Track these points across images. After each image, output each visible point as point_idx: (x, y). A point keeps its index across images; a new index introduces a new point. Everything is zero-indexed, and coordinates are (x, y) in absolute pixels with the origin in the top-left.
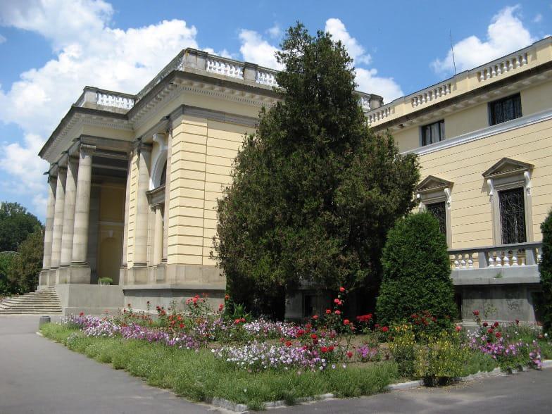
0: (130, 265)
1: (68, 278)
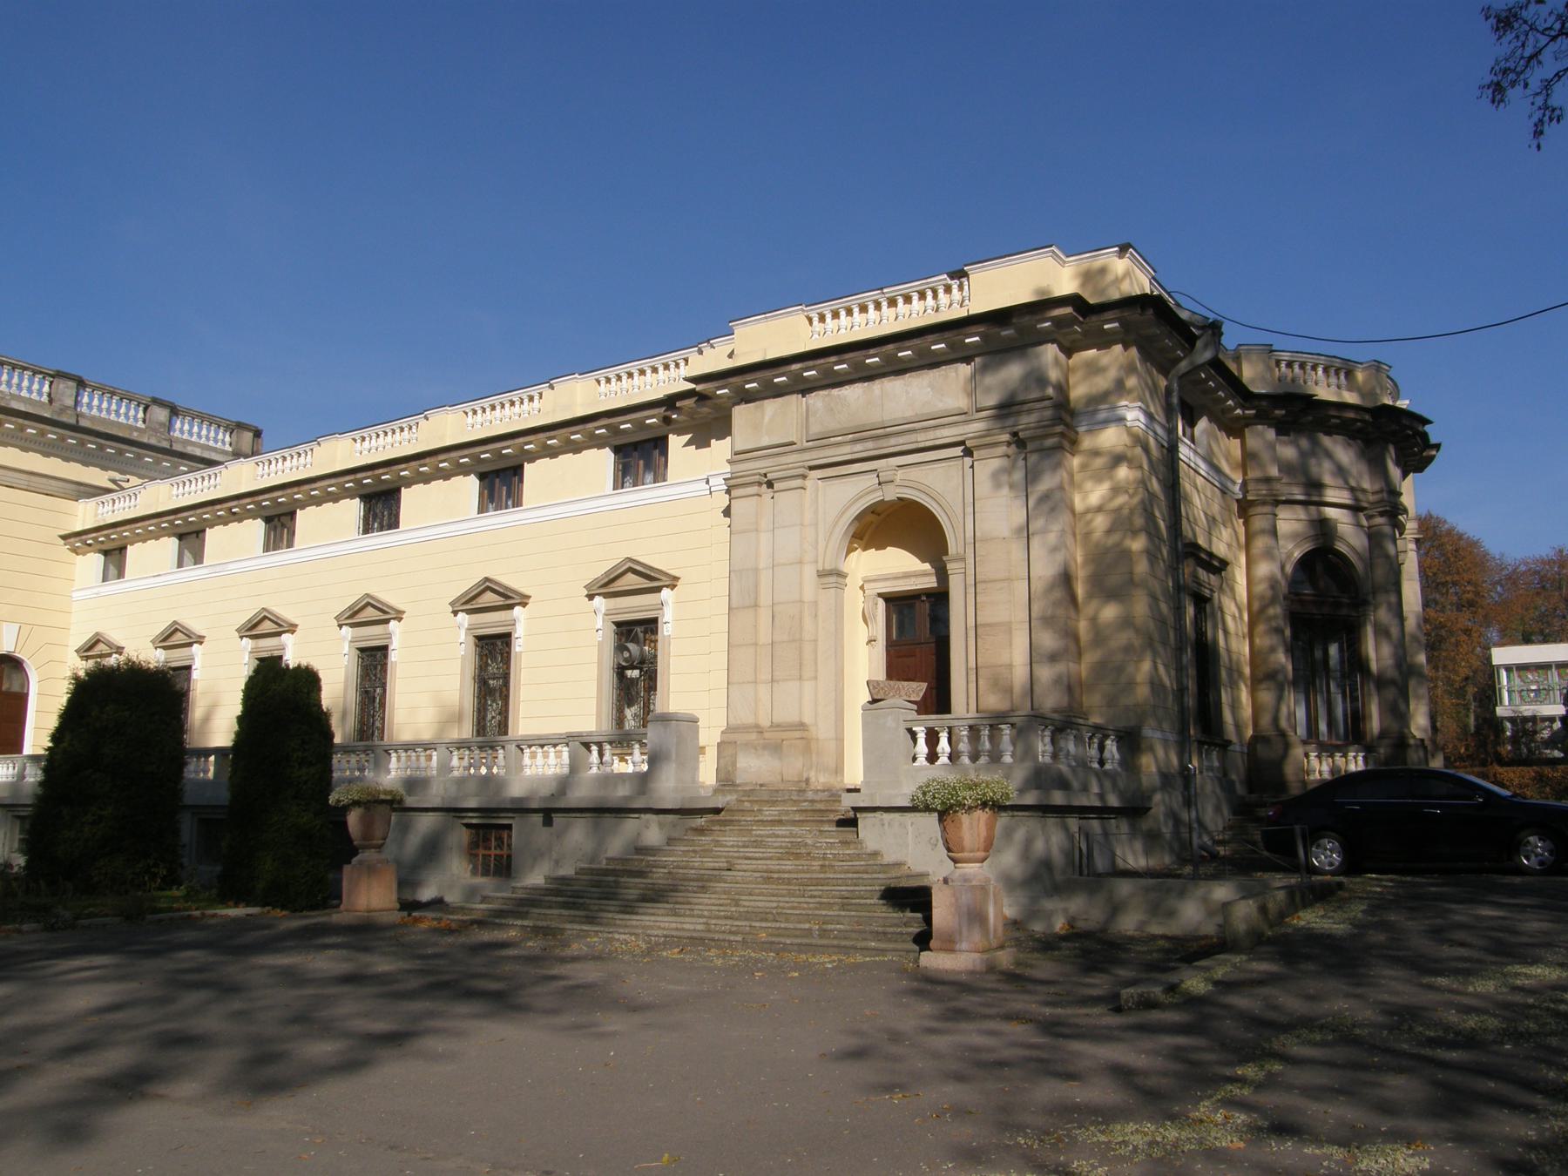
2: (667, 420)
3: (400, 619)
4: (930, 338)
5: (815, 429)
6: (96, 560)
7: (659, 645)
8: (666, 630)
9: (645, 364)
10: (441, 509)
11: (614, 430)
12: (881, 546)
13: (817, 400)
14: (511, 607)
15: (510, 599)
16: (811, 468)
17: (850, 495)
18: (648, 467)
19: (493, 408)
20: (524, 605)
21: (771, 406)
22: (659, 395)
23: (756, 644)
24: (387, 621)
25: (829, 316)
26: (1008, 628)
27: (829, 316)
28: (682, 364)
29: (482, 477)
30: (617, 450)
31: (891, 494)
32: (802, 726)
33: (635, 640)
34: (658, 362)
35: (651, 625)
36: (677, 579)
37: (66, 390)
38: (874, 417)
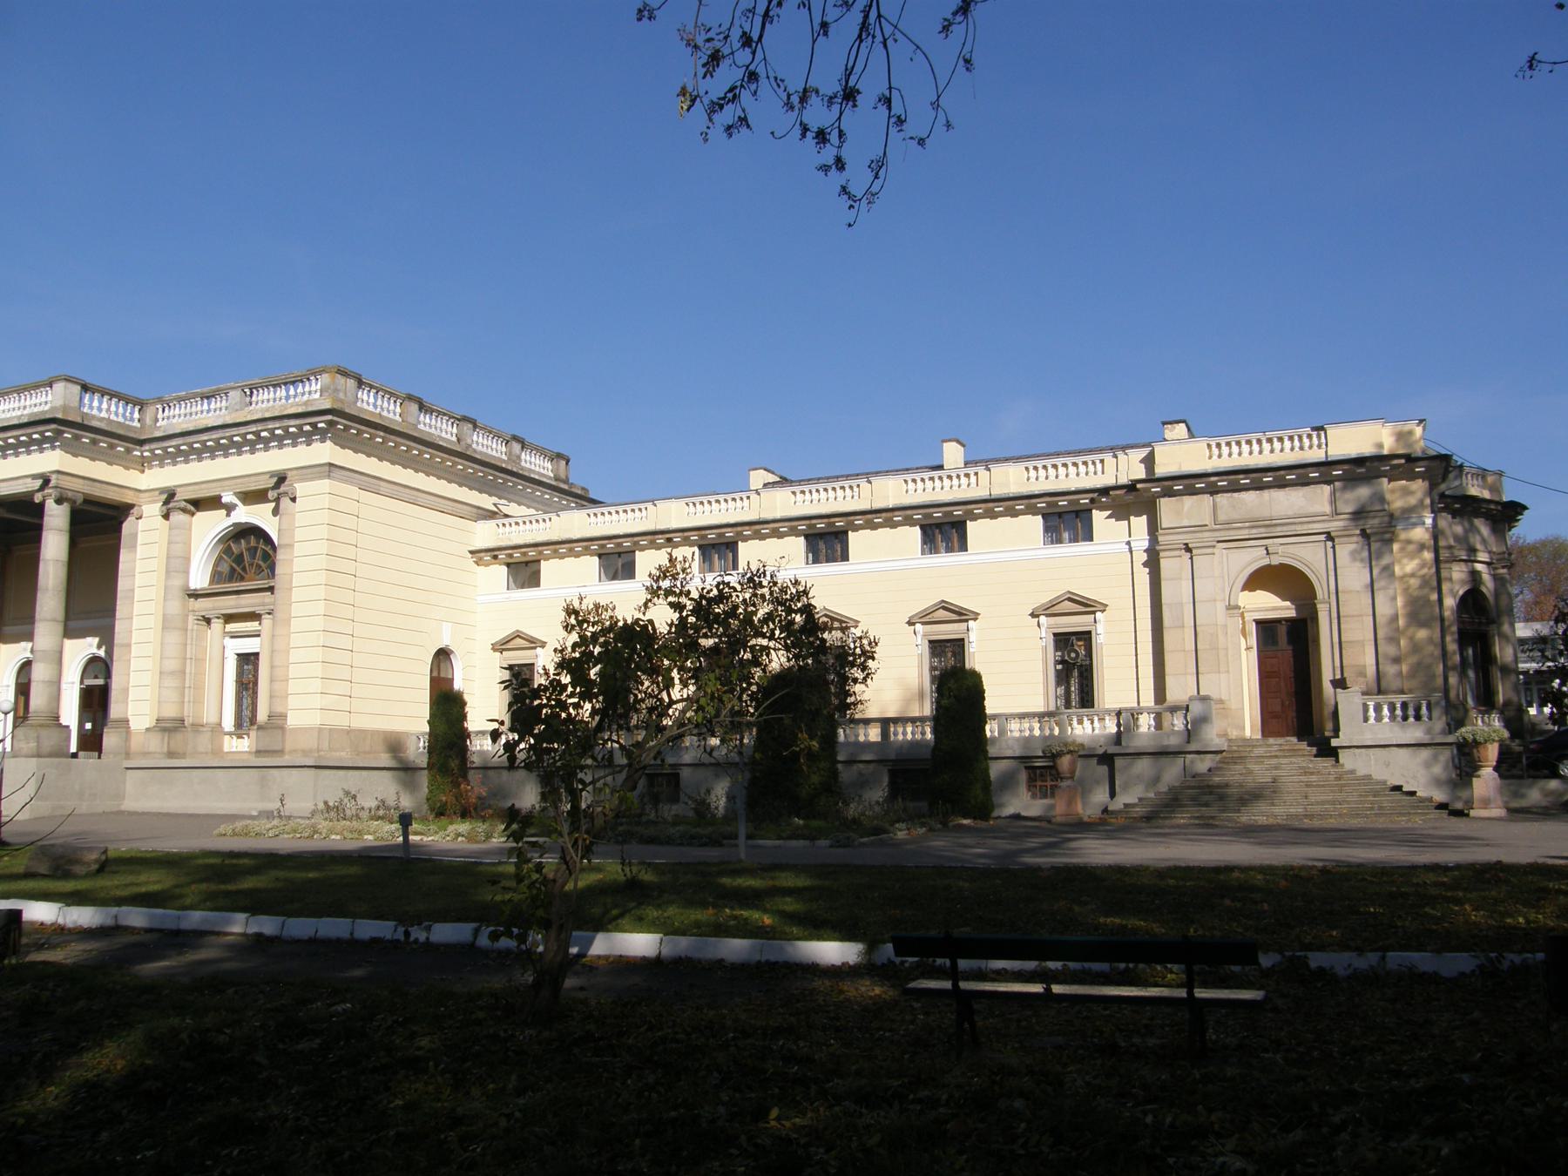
2: (1092, 501)
5: (1222, 517)
17: (1252, 558)
21: (1188, 501)
31: (1275, 561)
35: (1086, 637)
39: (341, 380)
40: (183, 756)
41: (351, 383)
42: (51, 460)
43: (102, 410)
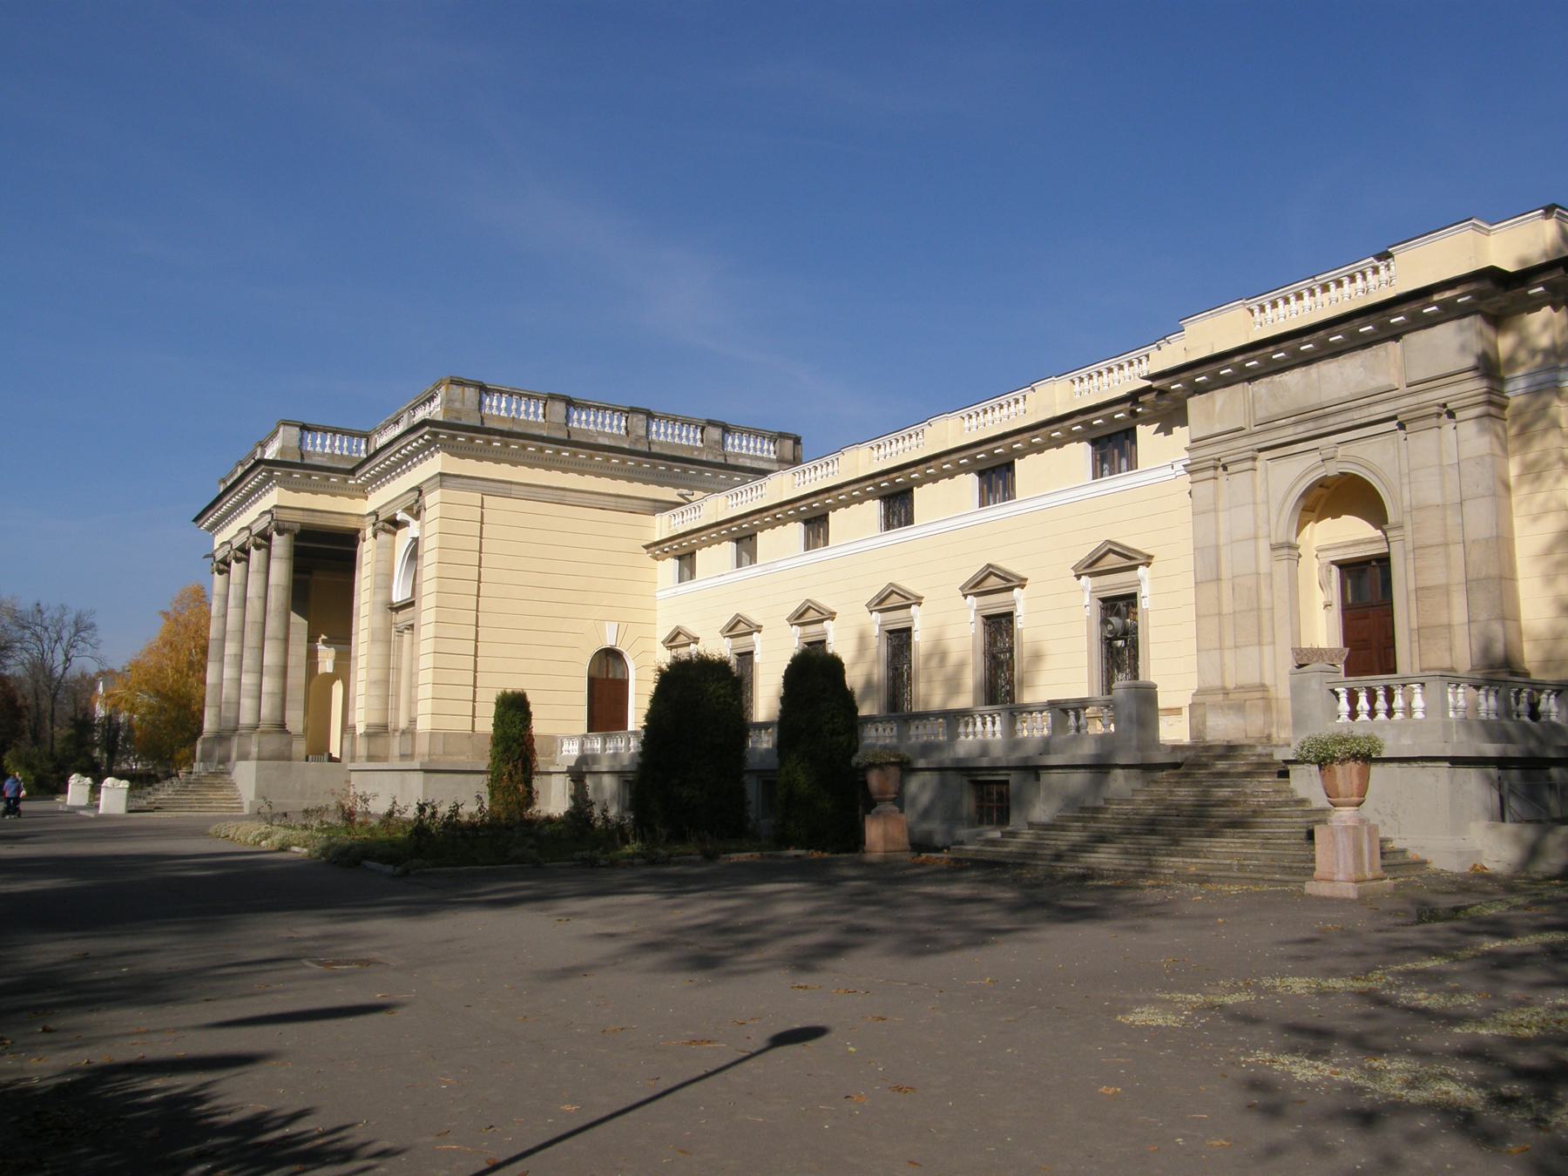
0: (360, 729)
1: (254, 750)
2: (1133, 413)
3: (920, 604)
4: (1357, 322)
5: (1261, 414)
6: (671, 565)
7: (1139, 617)
8: (1144, 603)
9: (1112, 363)
10: (947, 503)
11: (1088, 425)
12: (1336, 516)
13: (1261, 387)
14: (1011, 589)
15: (1011, 582)
16: (1260, 450)
18: (1121, 455)
19: (985, 412)
20: (1022, 587)
21: (1220, 396)
22: (1122, 393)
23: (1220, 614)
24: (909, 606)
25: (1268, 307)
26: (1446, 590)
27: (1268, 307)
28: (1144, 360)
29: (981, 474)
30: (1094, 442)
31: (1332, 470)
32: (1263, 687)
33: (1118, 614)
34: (1122, 360)
35: (1131, 599)
36: (1151, 557)
37: (639, 421)
38: (1313, 399)
39: (457, 391)
40: (385, 759)
41: (471, 393)
42: (274, 497)
43: (322, 447)
